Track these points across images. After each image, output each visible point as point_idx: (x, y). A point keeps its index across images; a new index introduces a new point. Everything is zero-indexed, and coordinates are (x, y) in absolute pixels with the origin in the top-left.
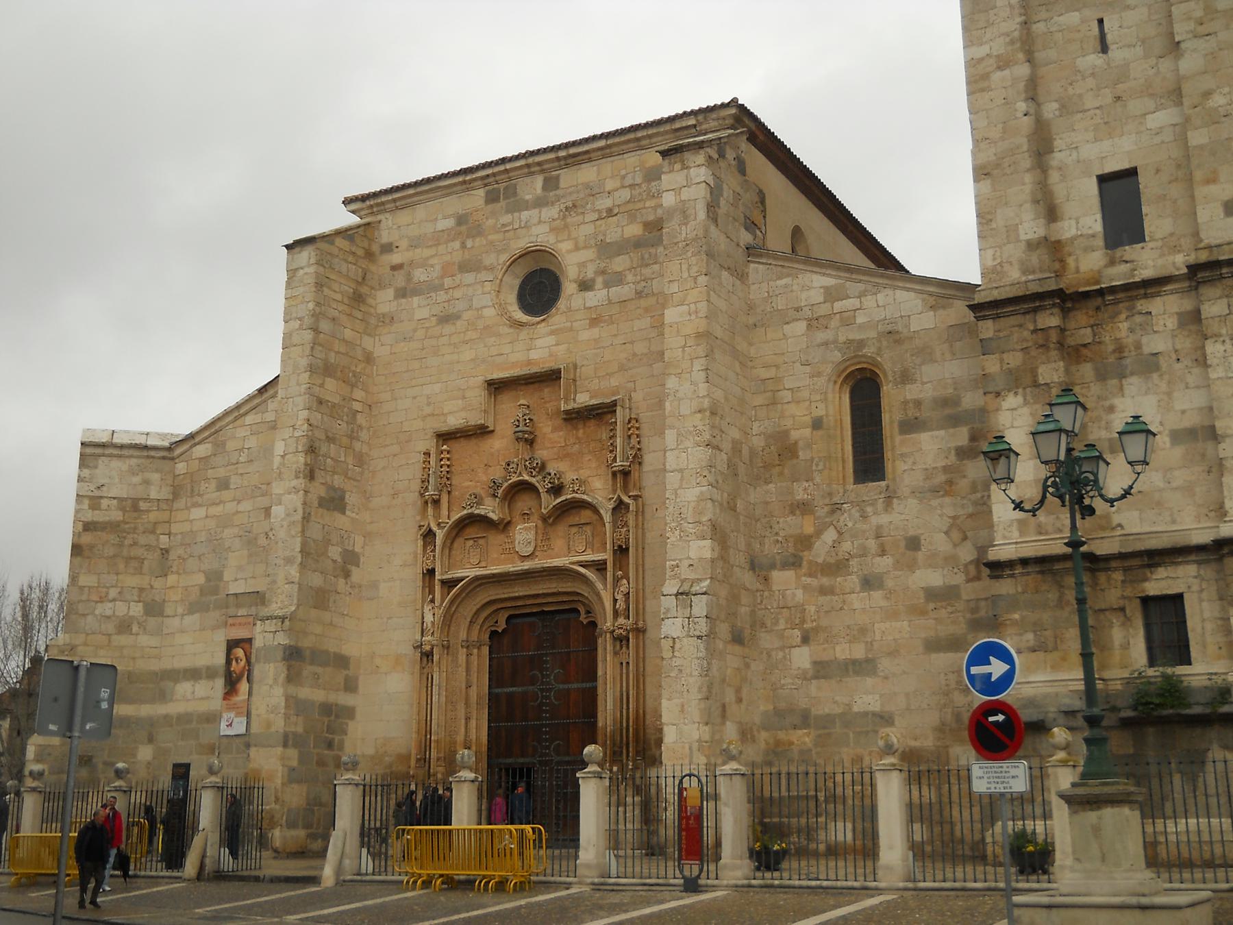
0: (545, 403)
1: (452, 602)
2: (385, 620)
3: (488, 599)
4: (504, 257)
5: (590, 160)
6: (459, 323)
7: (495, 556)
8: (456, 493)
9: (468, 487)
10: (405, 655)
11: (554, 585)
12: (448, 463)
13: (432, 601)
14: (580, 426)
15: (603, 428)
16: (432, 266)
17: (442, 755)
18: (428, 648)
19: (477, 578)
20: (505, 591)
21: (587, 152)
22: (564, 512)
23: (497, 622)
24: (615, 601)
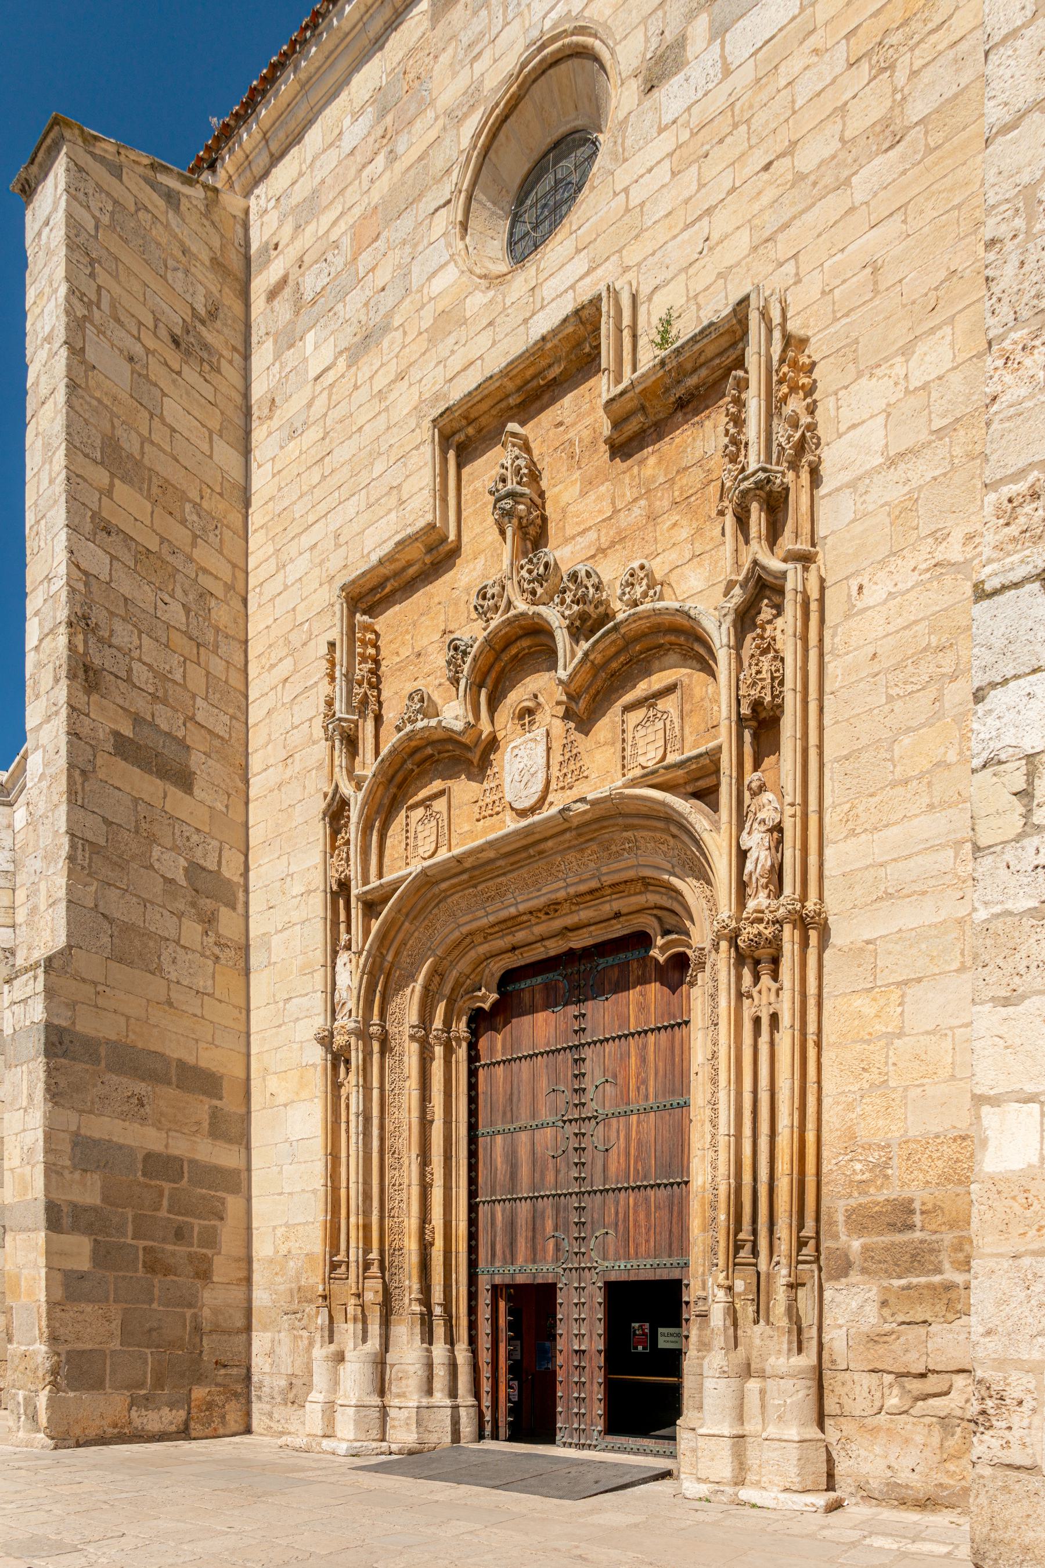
24: (743, 855)
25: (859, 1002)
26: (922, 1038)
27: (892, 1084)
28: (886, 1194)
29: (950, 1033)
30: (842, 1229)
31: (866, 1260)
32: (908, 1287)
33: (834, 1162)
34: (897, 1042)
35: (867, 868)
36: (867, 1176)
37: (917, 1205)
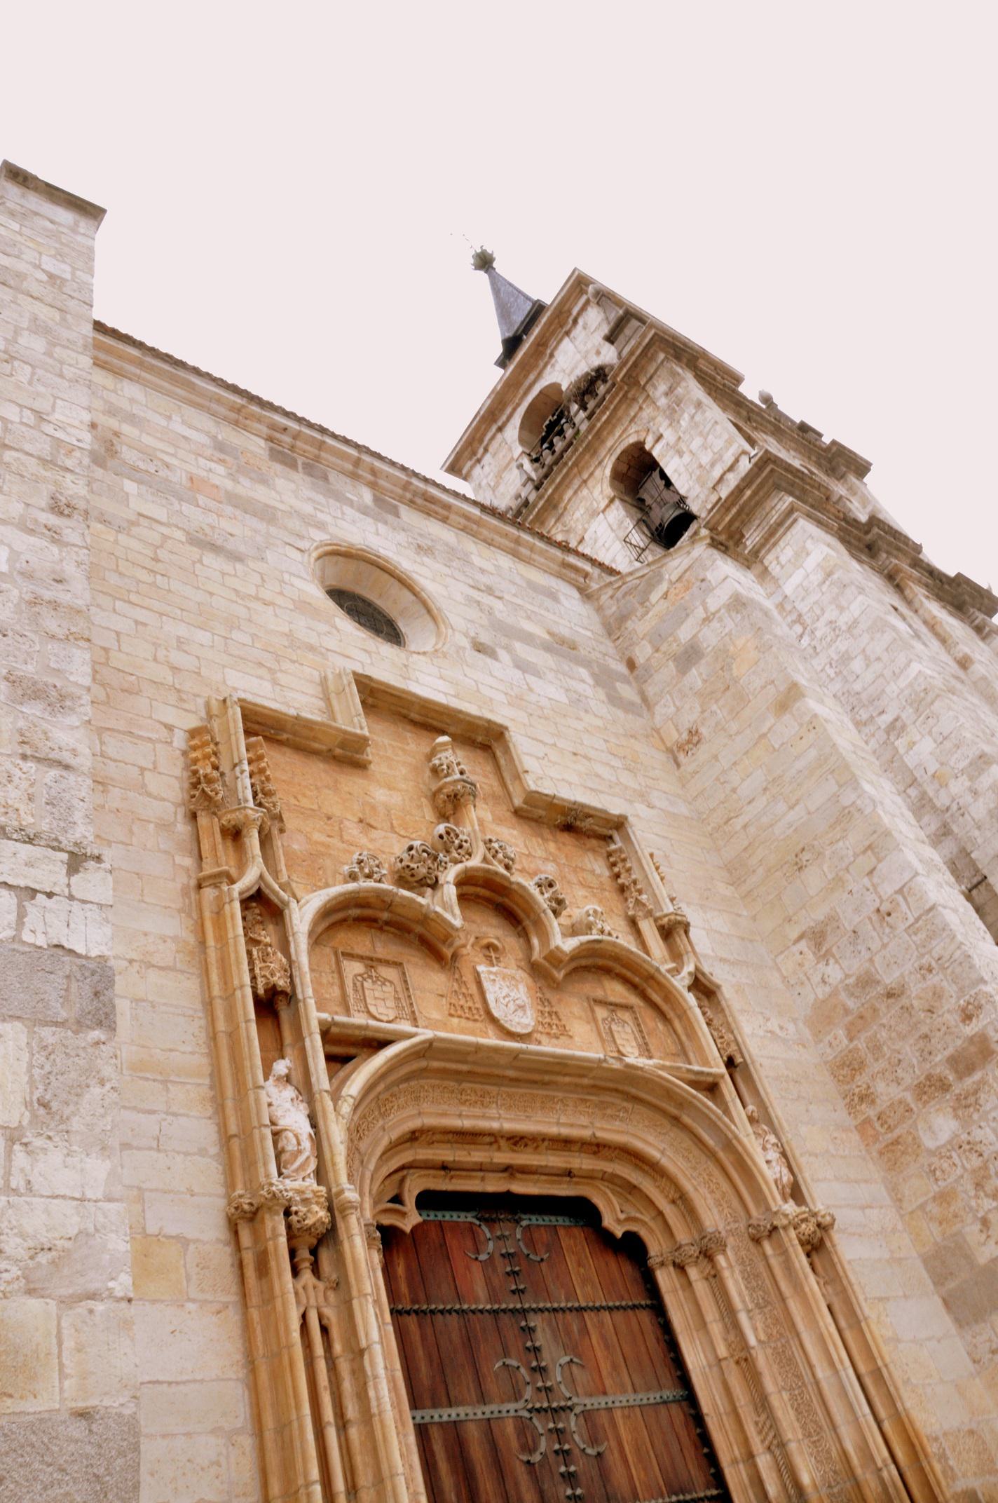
4: (319, 536)
5: (444, 520)
6: (238, 566)
7: (435, 1015)
10: (183, 1241)
11: (584, 1120)
16: (167, 466)
18: (319, 1214)
20: (465, 1109)
21: (447, 507)
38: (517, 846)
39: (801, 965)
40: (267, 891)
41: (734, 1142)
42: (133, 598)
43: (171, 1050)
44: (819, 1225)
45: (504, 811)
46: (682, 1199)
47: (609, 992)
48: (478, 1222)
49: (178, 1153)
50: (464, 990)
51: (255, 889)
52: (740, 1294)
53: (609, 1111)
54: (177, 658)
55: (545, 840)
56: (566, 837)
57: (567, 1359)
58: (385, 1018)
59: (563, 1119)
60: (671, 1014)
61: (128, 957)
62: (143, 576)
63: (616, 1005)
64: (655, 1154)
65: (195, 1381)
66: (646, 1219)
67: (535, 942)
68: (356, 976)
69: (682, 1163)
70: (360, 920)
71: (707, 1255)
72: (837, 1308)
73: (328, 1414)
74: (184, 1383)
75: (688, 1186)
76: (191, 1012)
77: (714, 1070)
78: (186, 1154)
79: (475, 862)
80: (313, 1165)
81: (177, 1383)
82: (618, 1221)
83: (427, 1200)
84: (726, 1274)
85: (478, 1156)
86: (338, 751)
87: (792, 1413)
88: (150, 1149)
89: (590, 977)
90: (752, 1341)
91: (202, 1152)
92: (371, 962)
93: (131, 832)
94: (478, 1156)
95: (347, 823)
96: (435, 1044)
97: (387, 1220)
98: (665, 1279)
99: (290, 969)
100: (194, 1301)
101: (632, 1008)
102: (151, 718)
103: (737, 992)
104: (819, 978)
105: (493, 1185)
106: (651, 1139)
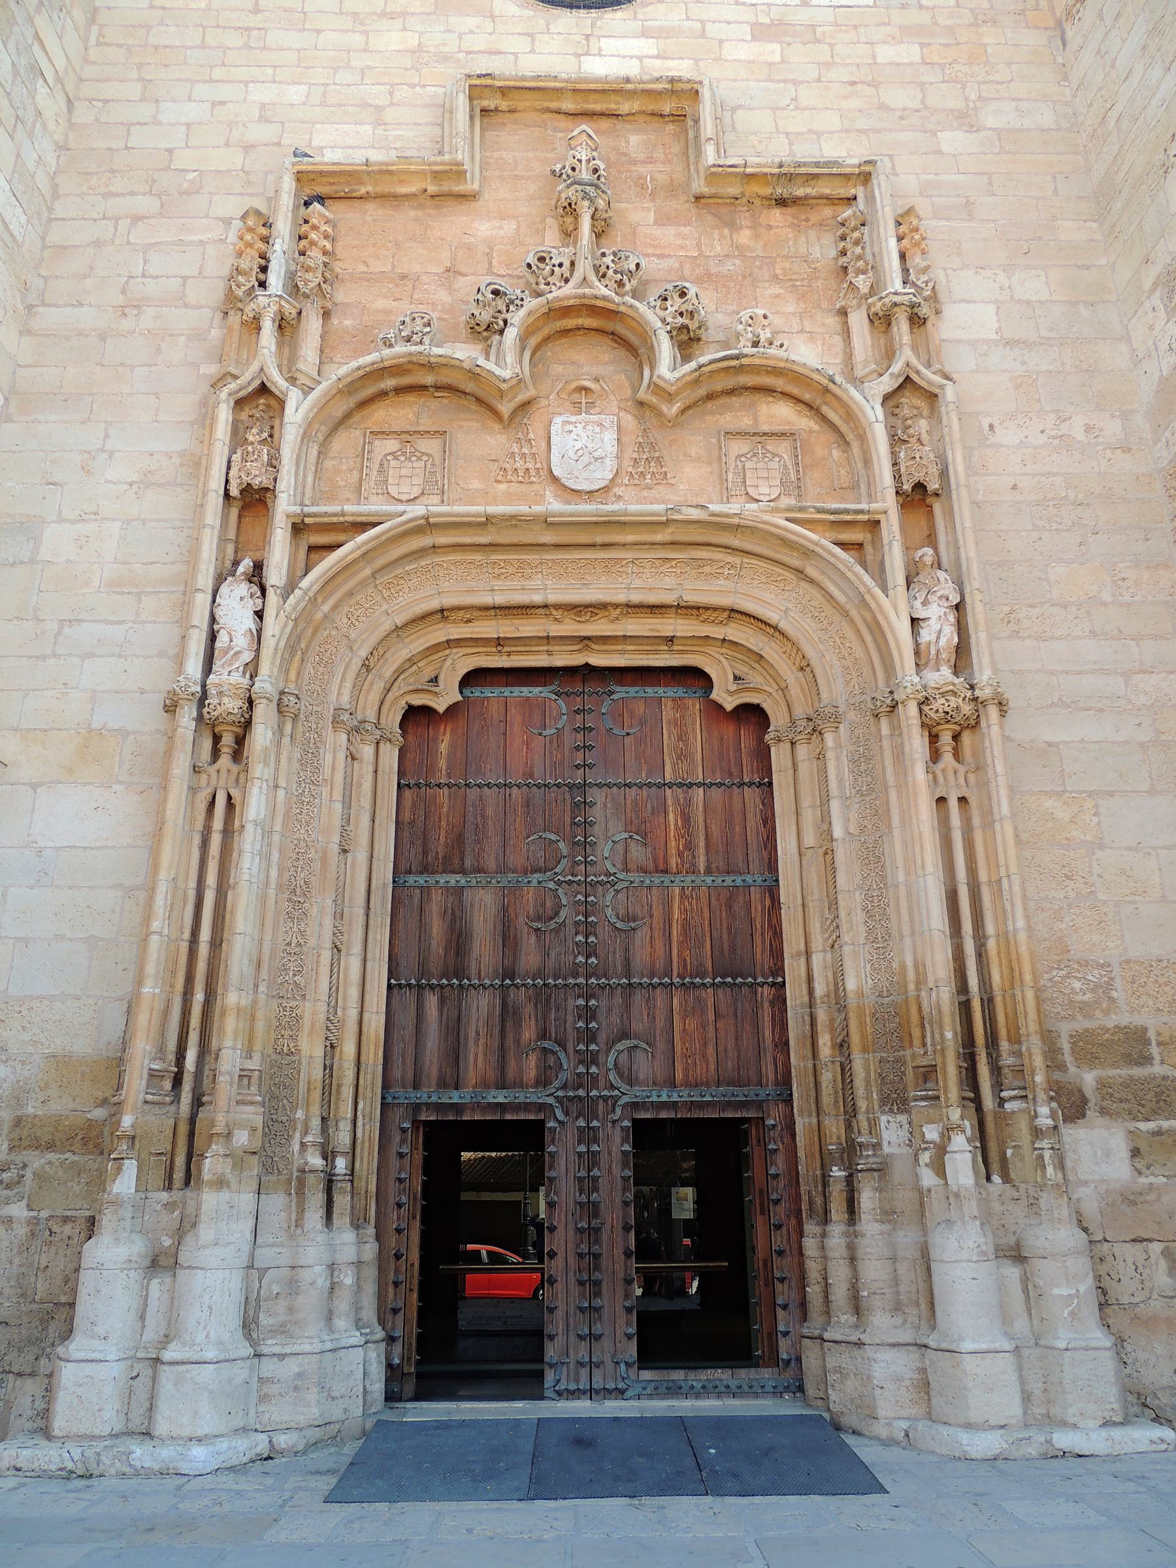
0: (635, 162)
1: (330, 581)
2: (53, 626)
3: (435, 604)
7: (476, 485)
8: (344, 322)
9: (387, 312)
10: (123, 733)
11: (670, 582)
12: (329, 247)
13: (257, 575)
14: (744, 219)
15: (812, 234)
17: (254, 1064)
19: (427, 525)
20: (497, 584)
22: (710, 397)
23: (435, 680)
25: (1049, 804)
26: (1125, 852)
27: (1101, 896)
28: (1112, 1021)
29: (1153, 853)
30: (1068, 1058)
31: (1103, 1099)
32: (1159, 1133)
33: (1047, 976)
34: (1099, 854)
35: (1037, 671)
36: (1088, 997)
37: (1151, 1034)
38: (682, 247)
39: (1151, 328)
40: (268, 384)
41: (867, 597)
42: (217, 73)
43: (152, 563)
44: (975, 699)
45: (680, 204)
46: (805, 667)
47: (762, 419)
48: (554, 697)
49: (137, 657)
50: (525, 450)
51: (257, 383)
52: (840, 781)
53: (707, 569)
54: (258, 133)
55: (734, 227)
56: (777, 215)
57: (626, 835)
58: (405, 497)
59: (637, 583)
60: (850, 437)
61: (129, 480)
62: (234, 40)
63: (765, 434)
64: (772, 616)
65: (107, 847)
66: (771, 690)
67: (647, 373)
68: (385, 456)
69: (809, 625)
70: (399, 390)
71: (817, 732)
72: (973, 801)
73: (211, 879)
74: (98, 848)
75: (811, 654)
76: (181, 524)
77: (874, 506)
78: (144, 657)
79: (569, 290)
80: (247, 656)
81: (91, 848)
82: (731, 693)
83: (473, 678)
84: (830, 755)
85: (528, 628)
86: (432, 189)
87: (859, 917)
88: (113, 655)
89: (735, 400)
90: (838, 832)
91: (162, 654)
92: (407, 436)
93: (159, 351)
94: (528, 628)
95: (425, 278)
96: (431, 520)
97: (417, 700)
98: (779, 756)
99: (273, 464)
100: (122, 782)
101: (793, 434)
102: (207, 216)
103: (1017, 387)
104: (1165, 346)
105: (562, 659)
106: (768, 597)
